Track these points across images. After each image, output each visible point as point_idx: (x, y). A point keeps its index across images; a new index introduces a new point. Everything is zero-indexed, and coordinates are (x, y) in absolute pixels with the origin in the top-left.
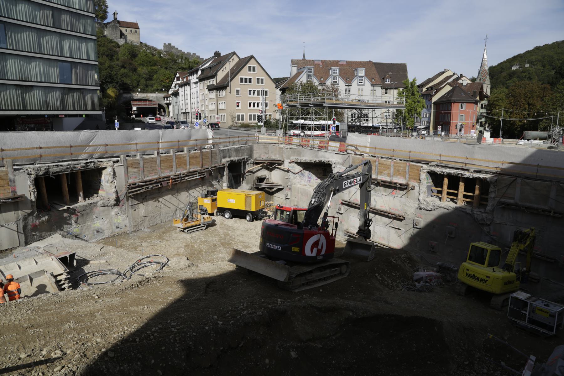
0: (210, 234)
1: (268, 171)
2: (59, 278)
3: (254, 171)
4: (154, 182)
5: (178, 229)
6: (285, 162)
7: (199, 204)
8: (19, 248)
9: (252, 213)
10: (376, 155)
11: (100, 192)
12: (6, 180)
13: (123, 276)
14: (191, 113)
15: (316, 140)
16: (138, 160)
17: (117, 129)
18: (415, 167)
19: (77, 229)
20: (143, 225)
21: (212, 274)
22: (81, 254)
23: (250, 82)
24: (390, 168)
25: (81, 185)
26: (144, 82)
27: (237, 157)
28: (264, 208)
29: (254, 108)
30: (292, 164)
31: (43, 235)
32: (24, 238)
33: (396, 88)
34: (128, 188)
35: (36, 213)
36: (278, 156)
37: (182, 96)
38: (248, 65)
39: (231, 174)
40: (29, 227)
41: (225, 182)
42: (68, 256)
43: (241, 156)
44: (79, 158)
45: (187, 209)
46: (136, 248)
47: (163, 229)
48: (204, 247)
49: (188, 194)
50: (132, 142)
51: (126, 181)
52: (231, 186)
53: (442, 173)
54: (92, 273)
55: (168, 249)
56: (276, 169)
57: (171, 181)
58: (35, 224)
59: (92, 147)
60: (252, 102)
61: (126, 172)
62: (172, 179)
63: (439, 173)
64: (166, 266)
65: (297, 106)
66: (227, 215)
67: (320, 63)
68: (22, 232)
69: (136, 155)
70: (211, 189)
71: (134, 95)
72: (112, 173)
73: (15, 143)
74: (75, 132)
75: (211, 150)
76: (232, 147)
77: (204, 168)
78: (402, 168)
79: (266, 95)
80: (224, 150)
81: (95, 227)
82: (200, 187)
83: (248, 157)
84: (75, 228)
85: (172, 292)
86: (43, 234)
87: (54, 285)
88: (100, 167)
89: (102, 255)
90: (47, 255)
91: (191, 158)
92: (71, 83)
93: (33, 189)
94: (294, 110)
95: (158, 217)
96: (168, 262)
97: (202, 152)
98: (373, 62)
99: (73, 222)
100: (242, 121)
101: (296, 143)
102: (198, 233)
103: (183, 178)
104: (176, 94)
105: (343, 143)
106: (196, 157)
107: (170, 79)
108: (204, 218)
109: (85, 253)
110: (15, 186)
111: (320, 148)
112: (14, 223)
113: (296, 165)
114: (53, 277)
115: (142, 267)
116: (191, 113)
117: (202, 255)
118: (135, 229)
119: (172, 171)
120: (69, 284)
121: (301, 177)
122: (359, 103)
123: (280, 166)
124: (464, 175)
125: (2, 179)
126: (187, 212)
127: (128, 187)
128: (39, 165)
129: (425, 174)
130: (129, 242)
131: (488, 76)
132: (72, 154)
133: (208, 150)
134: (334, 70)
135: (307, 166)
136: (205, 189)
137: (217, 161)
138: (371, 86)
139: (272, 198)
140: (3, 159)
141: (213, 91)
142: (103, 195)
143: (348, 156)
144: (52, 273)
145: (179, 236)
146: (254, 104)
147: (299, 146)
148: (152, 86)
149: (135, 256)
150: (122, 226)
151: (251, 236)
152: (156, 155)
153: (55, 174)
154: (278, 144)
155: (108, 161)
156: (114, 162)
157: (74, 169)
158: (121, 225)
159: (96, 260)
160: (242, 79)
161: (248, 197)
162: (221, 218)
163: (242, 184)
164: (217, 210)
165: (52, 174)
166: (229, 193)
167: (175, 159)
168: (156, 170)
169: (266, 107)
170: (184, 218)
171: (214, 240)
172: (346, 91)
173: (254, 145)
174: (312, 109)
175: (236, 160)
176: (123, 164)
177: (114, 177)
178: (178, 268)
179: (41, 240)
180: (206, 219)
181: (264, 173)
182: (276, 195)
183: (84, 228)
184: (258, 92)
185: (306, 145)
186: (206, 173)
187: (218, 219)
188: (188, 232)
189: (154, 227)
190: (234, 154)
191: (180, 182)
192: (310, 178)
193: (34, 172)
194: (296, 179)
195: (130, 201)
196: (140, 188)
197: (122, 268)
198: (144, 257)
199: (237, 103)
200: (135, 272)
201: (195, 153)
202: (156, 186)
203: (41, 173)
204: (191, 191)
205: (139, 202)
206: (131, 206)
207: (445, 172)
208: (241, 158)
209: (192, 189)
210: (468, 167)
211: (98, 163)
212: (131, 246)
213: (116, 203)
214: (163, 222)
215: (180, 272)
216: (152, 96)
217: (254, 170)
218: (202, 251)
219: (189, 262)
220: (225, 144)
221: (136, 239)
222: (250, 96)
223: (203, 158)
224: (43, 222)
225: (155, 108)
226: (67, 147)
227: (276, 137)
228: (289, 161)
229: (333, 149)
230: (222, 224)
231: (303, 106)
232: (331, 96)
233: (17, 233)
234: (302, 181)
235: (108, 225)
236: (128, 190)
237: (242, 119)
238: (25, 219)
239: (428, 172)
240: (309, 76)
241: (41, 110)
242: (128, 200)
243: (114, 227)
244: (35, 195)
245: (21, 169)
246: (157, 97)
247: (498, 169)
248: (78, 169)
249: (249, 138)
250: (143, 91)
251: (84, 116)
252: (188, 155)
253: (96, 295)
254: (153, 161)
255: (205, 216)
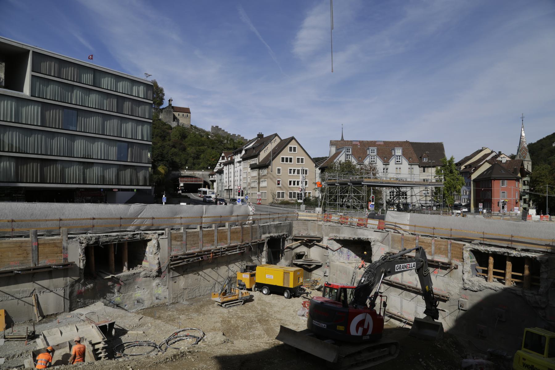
0: (248, 310)
1: (307, 248)
2: (97, 347)
3: (293, 248)
4: (195, 255)
5: (216, 303)
6: (324, 239)
7: (238, 278)
8: (63, 314)
9: (290, 289)
10: (416, 233)
11: (144, 263)
12: (60, 247)
13: (159, 349)
14: (234, 190)
15: (354, 218)
16: (182, 233)
17: (164, 203)
18: (457, 245)
19: (118, 298)
20: (181, 297)
21: (247, 351)
22: (120, 323)
23: (291, 161)
24: (431, 246)
25: (127, 255)
26: (192, 161)
27: (276, 233)
28: (302, 285)
29: (294, 186)
30: (331, 241)
31: (86, 302)
32: (69, 305)
33: (434, 167)
34: (170, 260)
35: (83, 281)
36: (317, 233)
37: (226, 174)
38: (289, 146)
39: (270, 250)
40: (75, 294)
41: (264, 258)
42: (108, 325)
43: (281, 232)
44: (127, 230)
45: (226, 283)
46: (173, 320)
47: (201, 302)
48: (241, 323)
49: (227, 268)
50: (177, 216)
51: (168, 253)
52: (270, 262)
53: (487, 252)
54: (129, 344)
55: (205, 323)
56: (315, 246)
57: (211, 255)
58: (81, 291)
59: (140, 220)
60: (293, 180)
61: (170, 244)
62: (213, 253)
63: (483, 252)
64: (202, 341)
65: (336, 184)
66: (265, 291)
67: (358, 143)
68: (68, 298)
69: (180, 229)
70: (250, 264)
71: (182, 172)
72: (156, 245)
73: (72, 213)
74: (126, 206)
75: (252, 226)
76: (272, 223)
77: (244, 243)
78: (443, 247)
79: (306, 174)
80: (264, 226)
81: (136, 297)
82: (239, 261)
83: (287, 233)
84: (117, 297)
85: (206, 368)
86: (87, 301)
87: (92, 354)
88: (145, 239)
89: (141, 326)
90: (88, 322)
91: (232, 233)
92: (126, 161)
93: (83, 257)
94: (334, 187)
95: (197, 290)
96: (204, 336)
97: (243, 228)
98: (410, 141)
99: (116, 290)
100: (282, 199)
101: (335, 220)
102: (235, 308)
103: (223, 253)
104: (221, 172)
105: (382, 221)
106: (237, 232)
107: (216, 158)
108: (242, 293)
109: (124, 323)
110: (67, 253)
111: (359, 225)
112: (61, 289)
113: (335, 242)
114: (91, 345)
115: (178, 341)
116: (234, 190)
117: (238, 331)
118: (174, 301)
119: (213, 245)
120: (105, 353)
121: (340, 254)
122: (398, 182)
123: (319, 243)
124: (510, 254)
125: (57, 247)
126: (226, 286)
127: (170, 259)
128: (90, 235)
129: (468, 252)
130: (167, 314)
131: (528, 153)
132: (121, 225)
133: (248, 226)
134: (372, 150)
135: (346, 243)
136: (244, 264)
137: (257, 237)
138: (409, 165)
139: (311, 275)
140: (60, 228)
141: (255, 170)
142: (146, 266)
143: (387, 234)
144: (91, 341)
145: (216, 310)
146: (294, 182)
147: (338, 223)
148: (199, 164)
149: (172, 329)
150: (162, 298)
151: (289, 313)
152: (198, 229)
153: (104, 244)
154: (317, 221)
155: (154, 233)
156: (159, 235)
157: (122, 240)
158: (161, 297)
159: (134, 330)
160: (283, 159)
161: (286, 273)
162: (259, 294)
163: (281, 261)
164: (255, 285)
165: (101, 243)
166: (267, 268)
167: (216, 233)
168: (198, 243)
169: (306, 185)
170: (222, 292)
171: (251, 316)
172: (384, 170)
173: (294, 222)
174: (350, 187)
175: (275, 236)
176: (167, 237)
177: (158, 249)
178: (214, 344)
179: (85, 307)
180: (244, 294)
181: (302, 249)
182: (314, 272)
183: (126, 298)
184: (298, 171)
185: (345, 223)
186: (246, 248)
187: (256, 294)
188: (225, 306)
189: (193, 300)
190: (274, 230)
191: (220, 256)
192: (348, 256)
193: (86, 241)
194: (334, 257)
195: (171, 273)
196: (182, 261)
197: (159, 340)
198: (181, 330)
199: (278, 181)
200: (171, 346)
201: (236, 229)
202: (197, 259)
203: (91, 242)
204: (231, 266)
205: (179, 275)
206: (172, 278)
207: (490, 251)
208: (281, 234)
209: (232, 263)
210: (514, 245)
211: (144, 235)
212: (169, 318)
213: (158, 274)
214: (201, 295)
215: (216, 347)
216: (199, 174)
217: (293, 247)
218: (238, 326)
219: (224, 337)
220: (266, 220)
221: (174, 311)
222: (290, 174)
223: (244, 233)
224: (88, 290)
225: (201, 184)
226: (117, 219)
227: (316, 215)
228: (328, 238)
229: (372, 226)
230: (259, 300)
231: (341, 184)
232: (369, 175)
233: (63, 298)
234: (341, 258)
235: (149, 296)
236: (170, 262)
237: (283, 197)
238: (72, 285)
239: (471, 251)
240: (347, 156)
241: (98, 184)
242: (169, 272)
243: (154, 298)
244: (84, 263)
245: (74, 238)
246: (202, 174)
247: (548, 248)
248: (125, 240)
249: (289, 215)
250: (190, 169)
251: (135, 190)
252: (229, 230)
253: (130, 367)
254: (196, 235)
255: (244, 291)
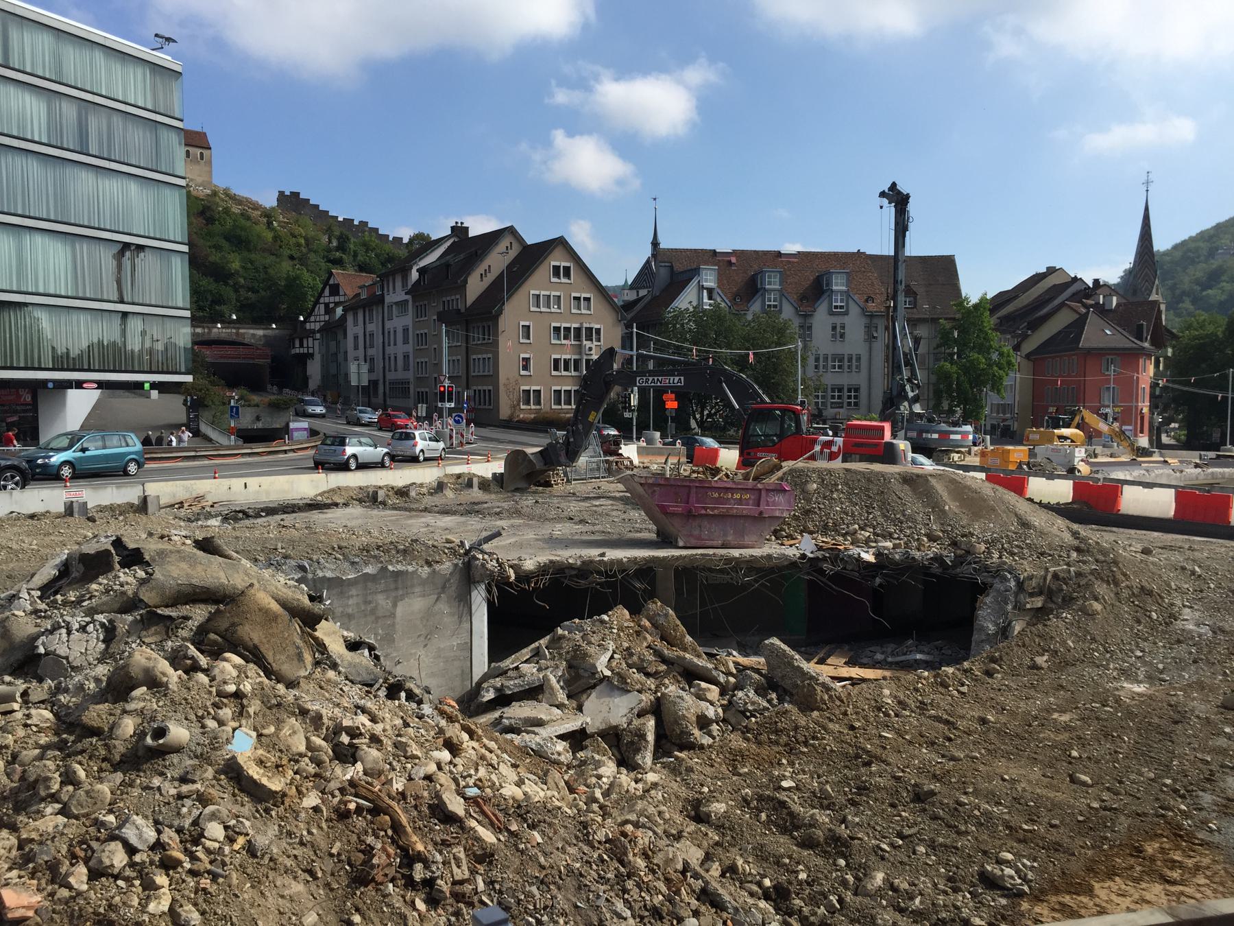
14: (384, 382)
116: (384, 382)
199: (527, 360)
216: (253, 335)
237: (538, 402)
246: (264, 336)
251: (147, 386)
